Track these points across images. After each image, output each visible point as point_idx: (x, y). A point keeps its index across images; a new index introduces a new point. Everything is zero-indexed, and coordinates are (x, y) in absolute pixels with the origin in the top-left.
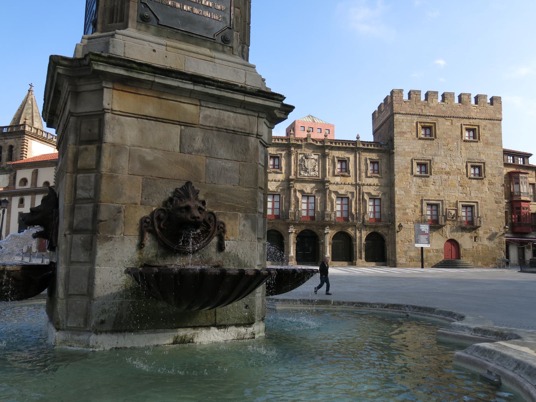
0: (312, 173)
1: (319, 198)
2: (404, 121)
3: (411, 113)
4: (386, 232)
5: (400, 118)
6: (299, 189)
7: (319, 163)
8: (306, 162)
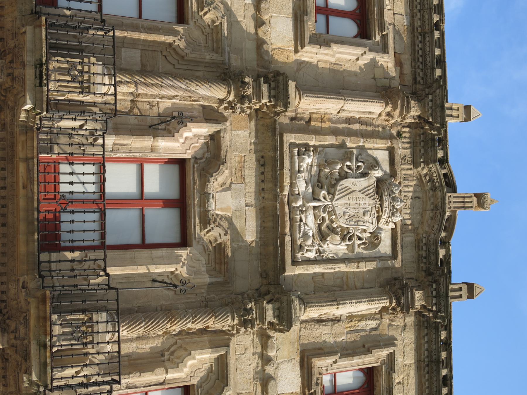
0: (310, 222)
1: (183, 271)
6: (226, 140)
7: (359, 259)
8: (364, 182)
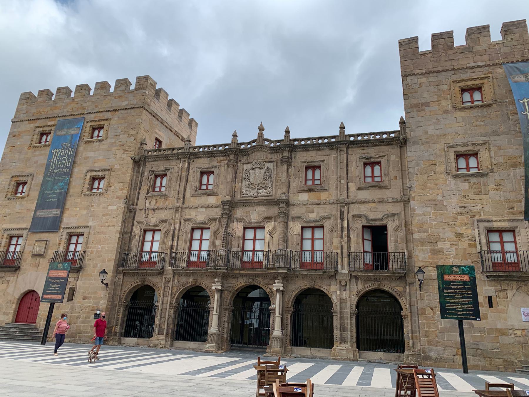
2: (423, 85)
3: (436, 69)
4: (400, 289)
5: (416, 81)
